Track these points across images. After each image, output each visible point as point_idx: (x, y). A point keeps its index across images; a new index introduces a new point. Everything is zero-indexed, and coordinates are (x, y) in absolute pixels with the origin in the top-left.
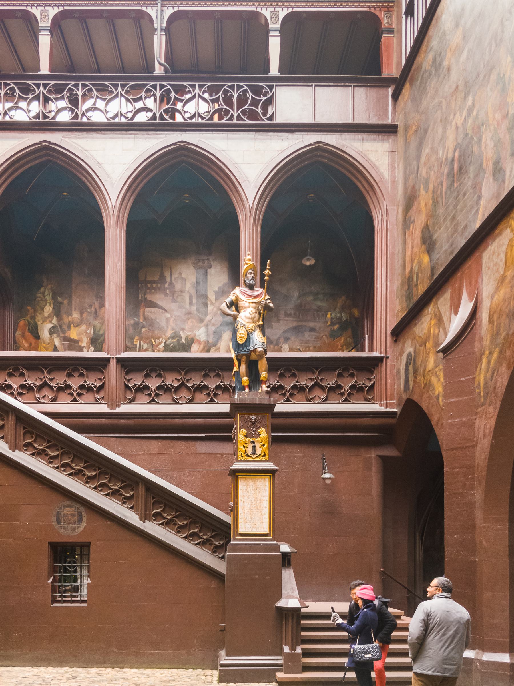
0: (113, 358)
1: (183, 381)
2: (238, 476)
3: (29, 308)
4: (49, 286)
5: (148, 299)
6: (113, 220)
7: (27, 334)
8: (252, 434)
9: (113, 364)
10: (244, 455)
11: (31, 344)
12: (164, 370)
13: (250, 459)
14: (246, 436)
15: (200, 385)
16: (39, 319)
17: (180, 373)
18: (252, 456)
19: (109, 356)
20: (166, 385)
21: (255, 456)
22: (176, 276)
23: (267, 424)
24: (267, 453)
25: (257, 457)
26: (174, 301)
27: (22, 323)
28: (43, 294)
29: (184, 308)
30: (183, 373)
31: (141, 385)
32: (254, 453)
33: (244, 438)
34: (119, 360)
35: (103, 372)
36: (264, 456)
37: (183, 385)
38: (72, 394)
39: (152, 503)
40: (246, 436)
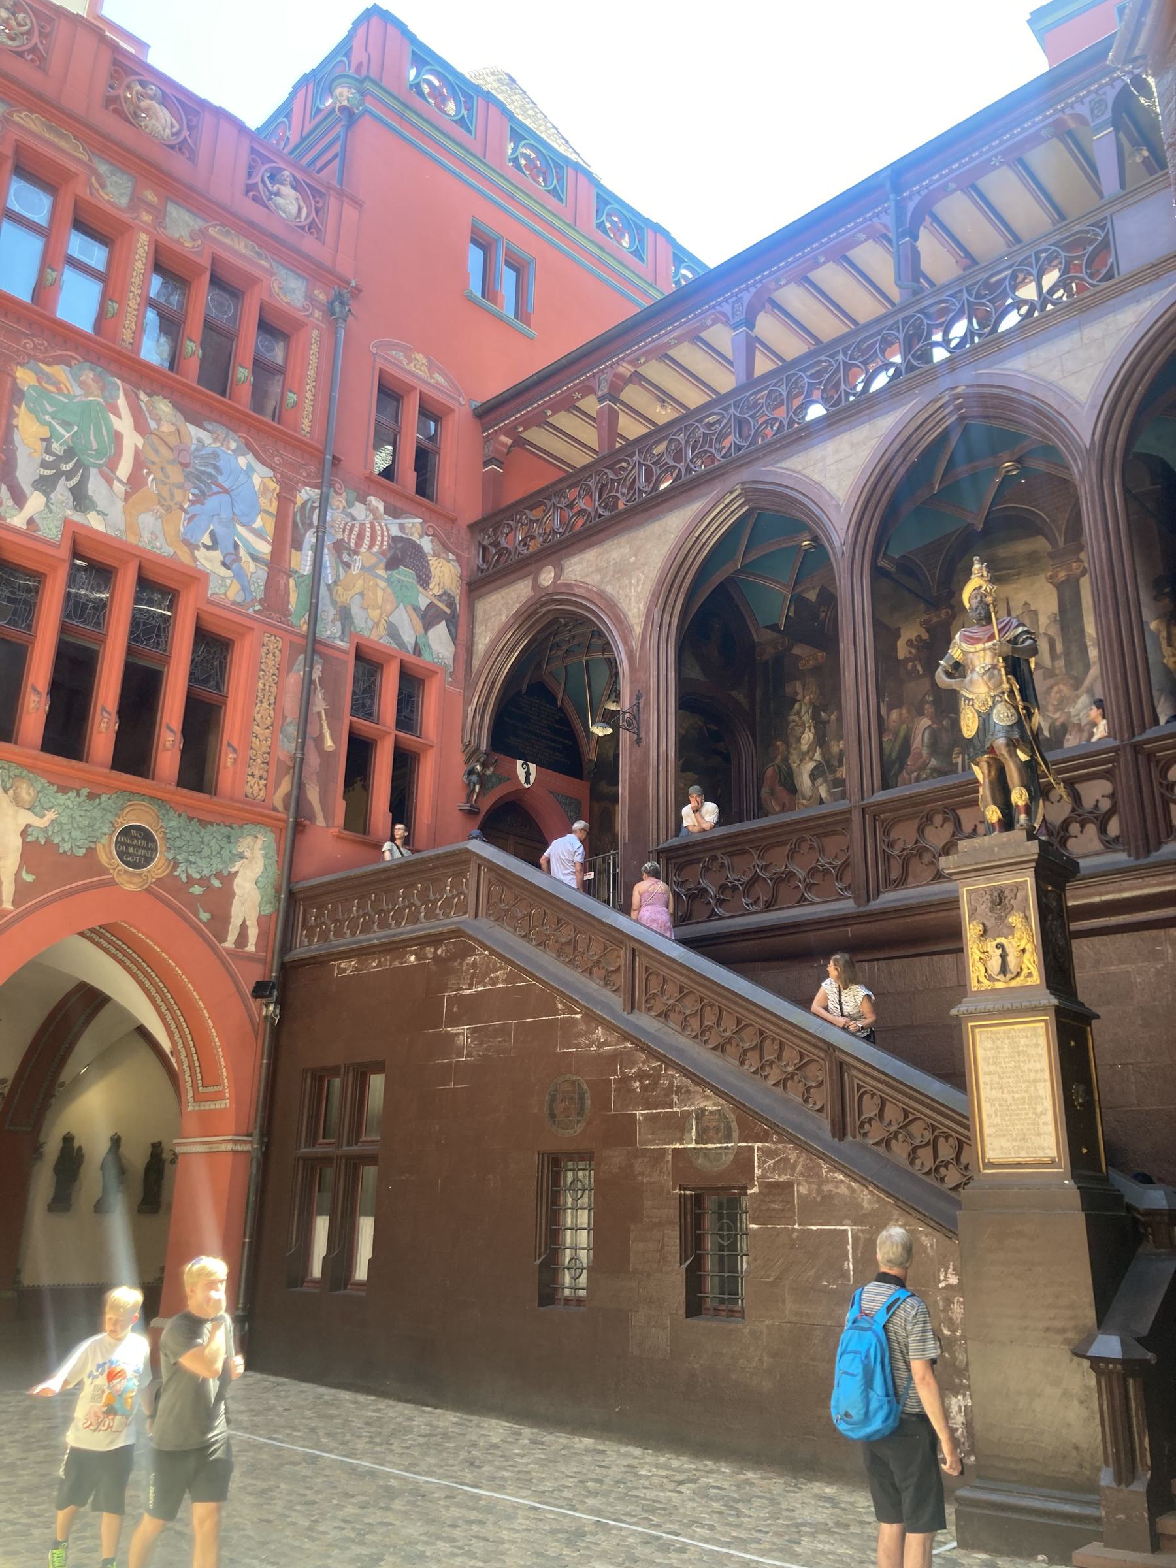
3: (779, 743)
4: (807, 698)
7: (778, 788)
9: (856, 816)
11: (784, 806)
13: (999, 985)
18: (1001, 977)
28: (798, 713)
32: (1004, 969)
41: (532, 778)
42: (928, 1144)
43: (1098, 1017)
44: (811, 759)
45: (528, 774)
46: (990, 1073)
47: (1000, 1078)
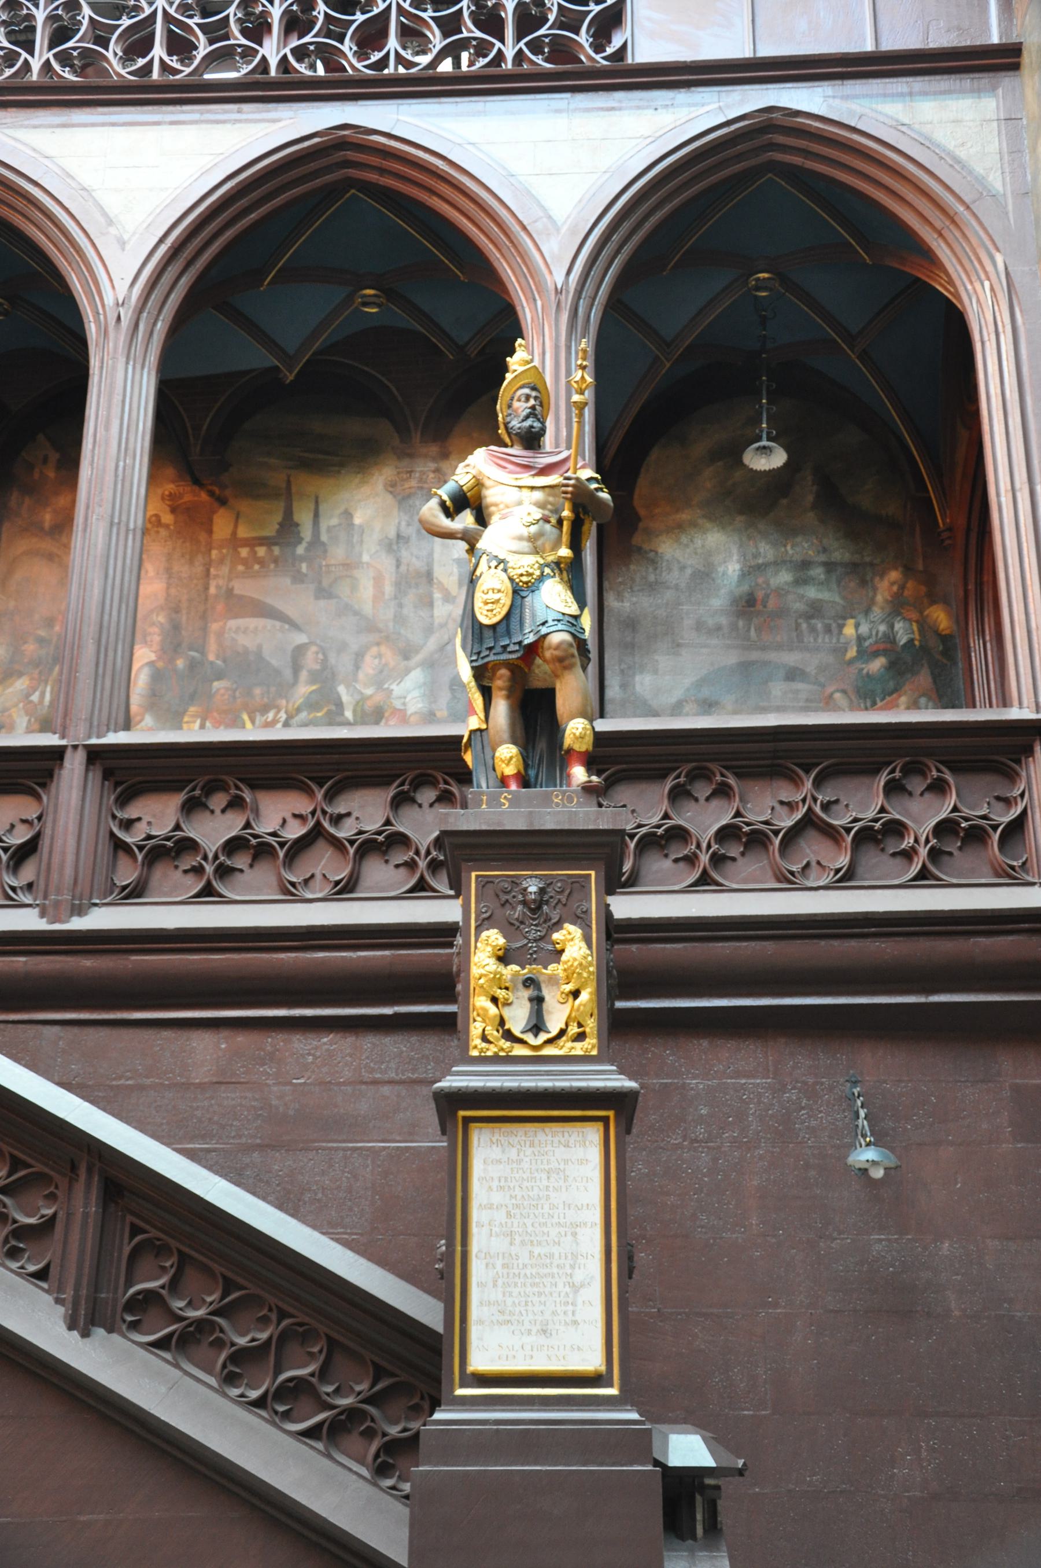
0: (75, 747)
1: (318, 824)
2: (467, 1121)
5: (236, 592)
6: (118, 339)
8: (529, 949)
9: (74, 765)
10: (492, 1032)
12: (254, 786)
13: (519, 1051)
14: (504, 958)
15: (379, 833)
17: (310, 793)
18: (529, 1038)
19: (64, 742)
20: (256, 836)
22: (334, 521)
23: (587, 912)
24: (591, 1025)
25: (550, 1041)
26: (323, 593)
29: (356, 613)
30: (320, 795)
31: (168, 839)
32: (537, 1026)
33: (493, 965)
34: (95, 755)
35: (38, 798)
36: (581, 1037)
37: (316, 834)
39: (127, 1250)
40: (504, 958)
46: (490, 1207)
47: (509, 1215)
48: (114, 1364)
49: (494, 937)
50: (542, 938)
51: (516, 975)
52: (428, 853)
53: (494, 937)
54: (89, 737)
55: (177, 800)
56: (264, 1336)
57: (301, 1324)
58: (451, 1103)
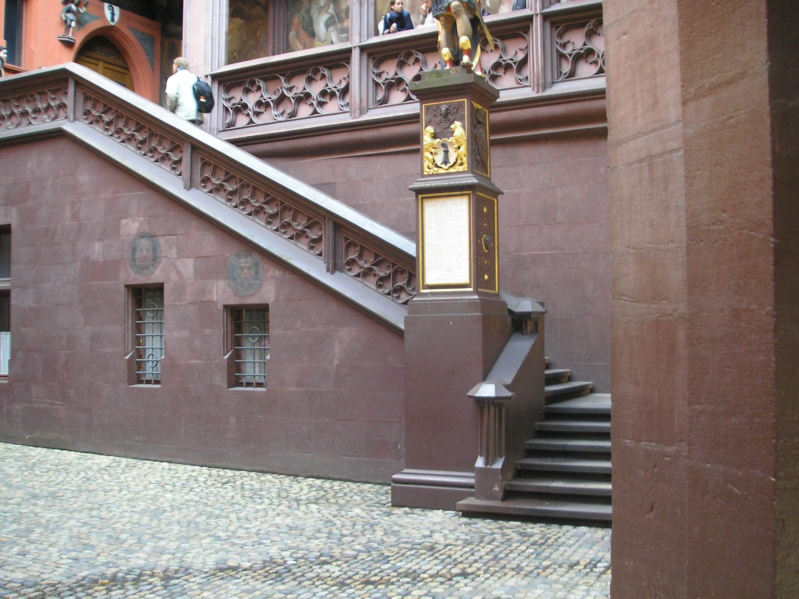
0: (355, 47)
7: (302, 32)
9: (356, 54)
13: (441, 171)
14: (435, 136)
16: (314, 11)
18: (444, 166)
21: (448, 165)
23: (464, 116)
24: (465, 159)
27: (296, 20)
32: (446, 162)
34: (363, 49)
36: (462, 164)
38: (312, 104)
41: (116, 18)
42: (389, 275)
43: (502, 193)
44: (326, 12)
45: (113, 14)
48: (343, 284)
49: (430, 129)
50: (448, 127)
51: (439, 142)
52: (489, 72)
53: (430, 129)
54: (360, 42)
55: (395, 61)
56: (388, 272)
57: (400, 268)
58: (418, 191)
